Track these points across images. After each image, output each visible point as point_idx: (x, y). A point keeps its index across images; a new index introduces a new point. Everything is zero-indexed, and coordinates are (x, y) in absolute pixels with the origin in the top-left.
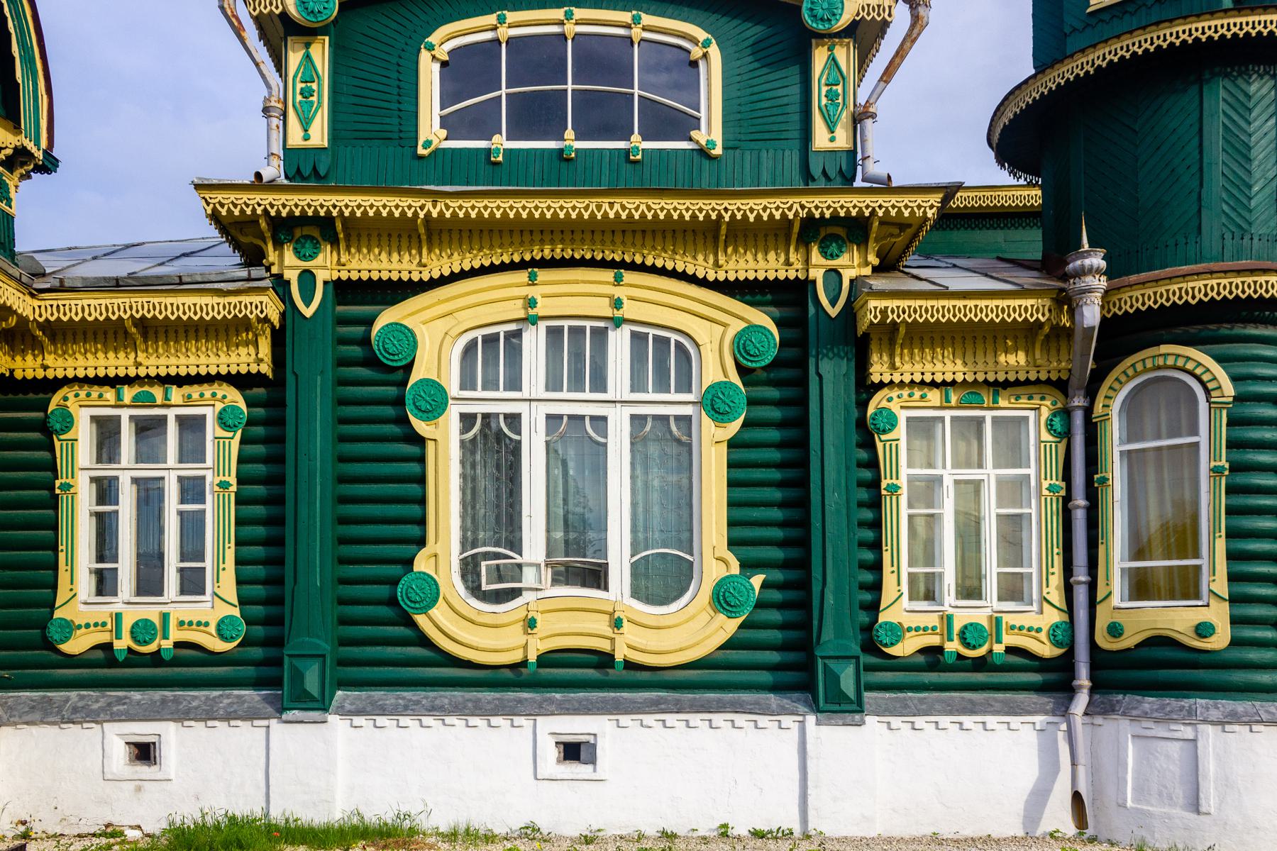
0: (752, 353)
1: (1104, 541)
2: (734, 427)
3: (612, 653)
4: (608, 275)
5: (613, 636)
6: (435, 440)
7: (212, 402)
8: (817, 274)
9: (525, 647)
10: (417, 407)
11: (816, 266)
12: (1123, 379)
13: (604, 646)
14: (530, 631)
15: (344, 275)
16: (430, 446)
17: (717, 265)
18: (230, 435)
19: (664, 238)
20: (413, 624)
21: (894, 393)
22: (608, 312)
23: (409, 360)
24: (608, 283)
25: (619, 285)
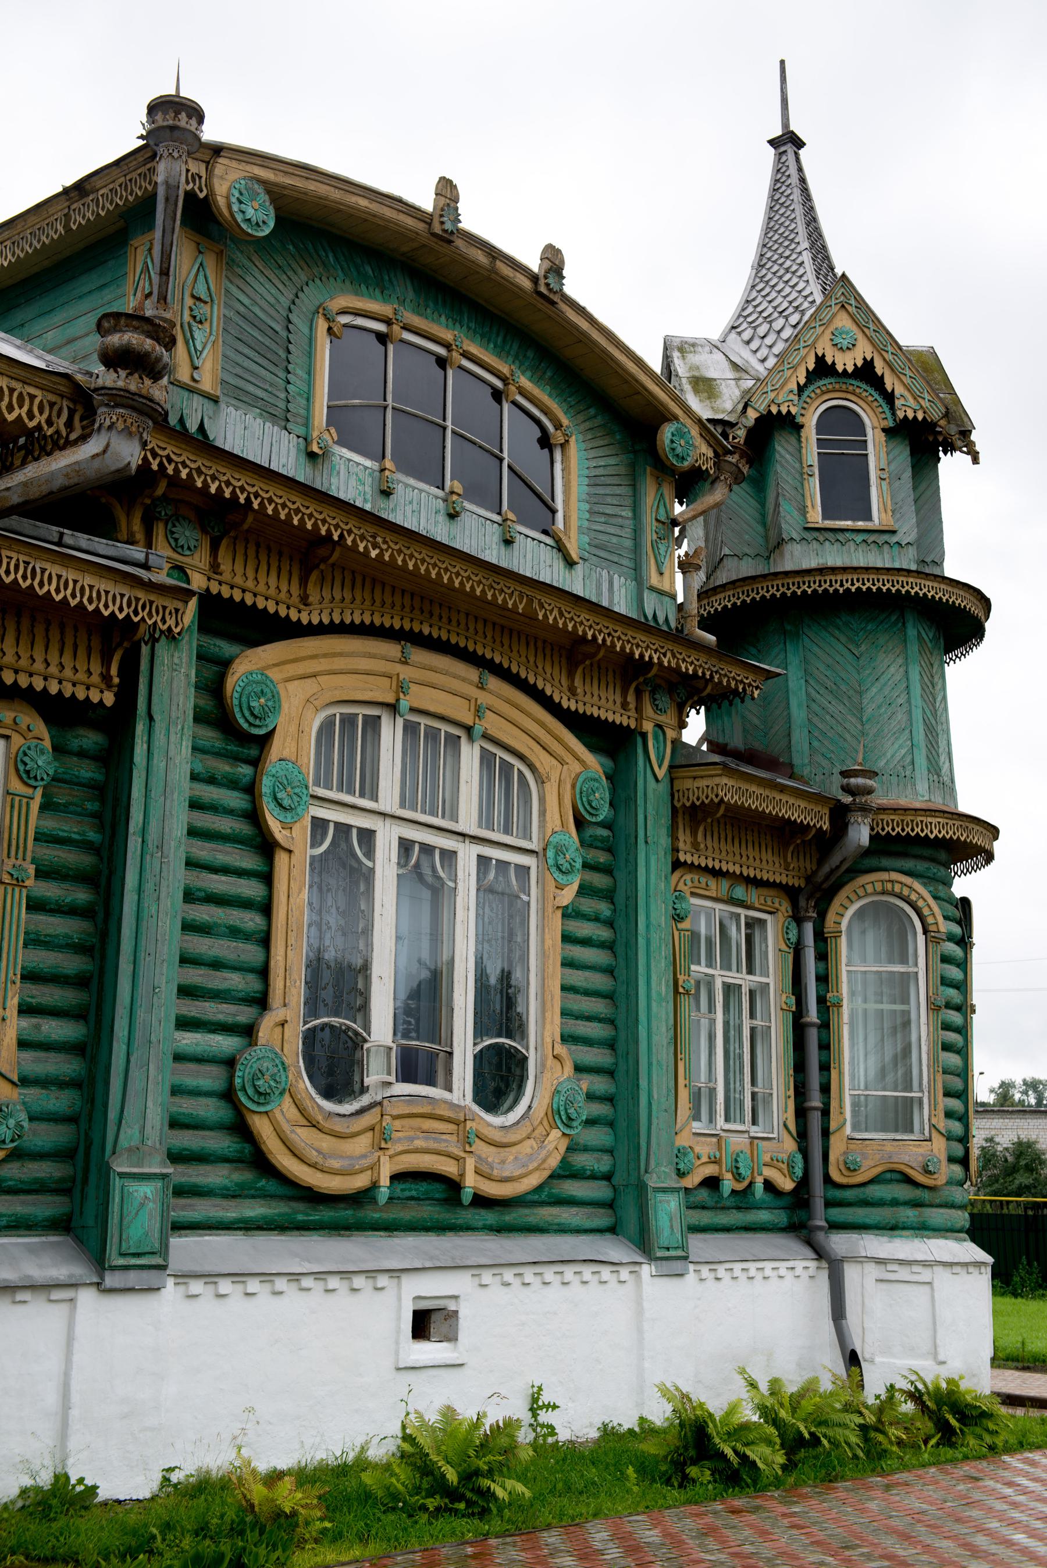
0: (594, 804)
1: (837, 1065)
2: (567, 896)
3: (457, 1179)
4: (472, 673)
5: (463, 1154)
6: (290, 852)
7: (7, 732)
8: (648, 727)
9: (374, 1167)
10: (276, 799)
11: (649, 719)
12: (853, 897)
13: (449, 1168)
14: (383, 1145)
15: (215, 589)
16: (281, 859)
17: (572, 691)
18: (29, 791)
19: (528, 644)
20: (241, 1129)
21: (688, 877)
22: (468, 719)
23: (271, 728)
24: (471, 683)
25: (482, 688)
